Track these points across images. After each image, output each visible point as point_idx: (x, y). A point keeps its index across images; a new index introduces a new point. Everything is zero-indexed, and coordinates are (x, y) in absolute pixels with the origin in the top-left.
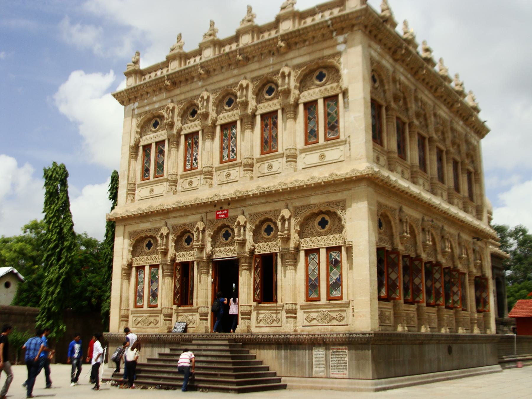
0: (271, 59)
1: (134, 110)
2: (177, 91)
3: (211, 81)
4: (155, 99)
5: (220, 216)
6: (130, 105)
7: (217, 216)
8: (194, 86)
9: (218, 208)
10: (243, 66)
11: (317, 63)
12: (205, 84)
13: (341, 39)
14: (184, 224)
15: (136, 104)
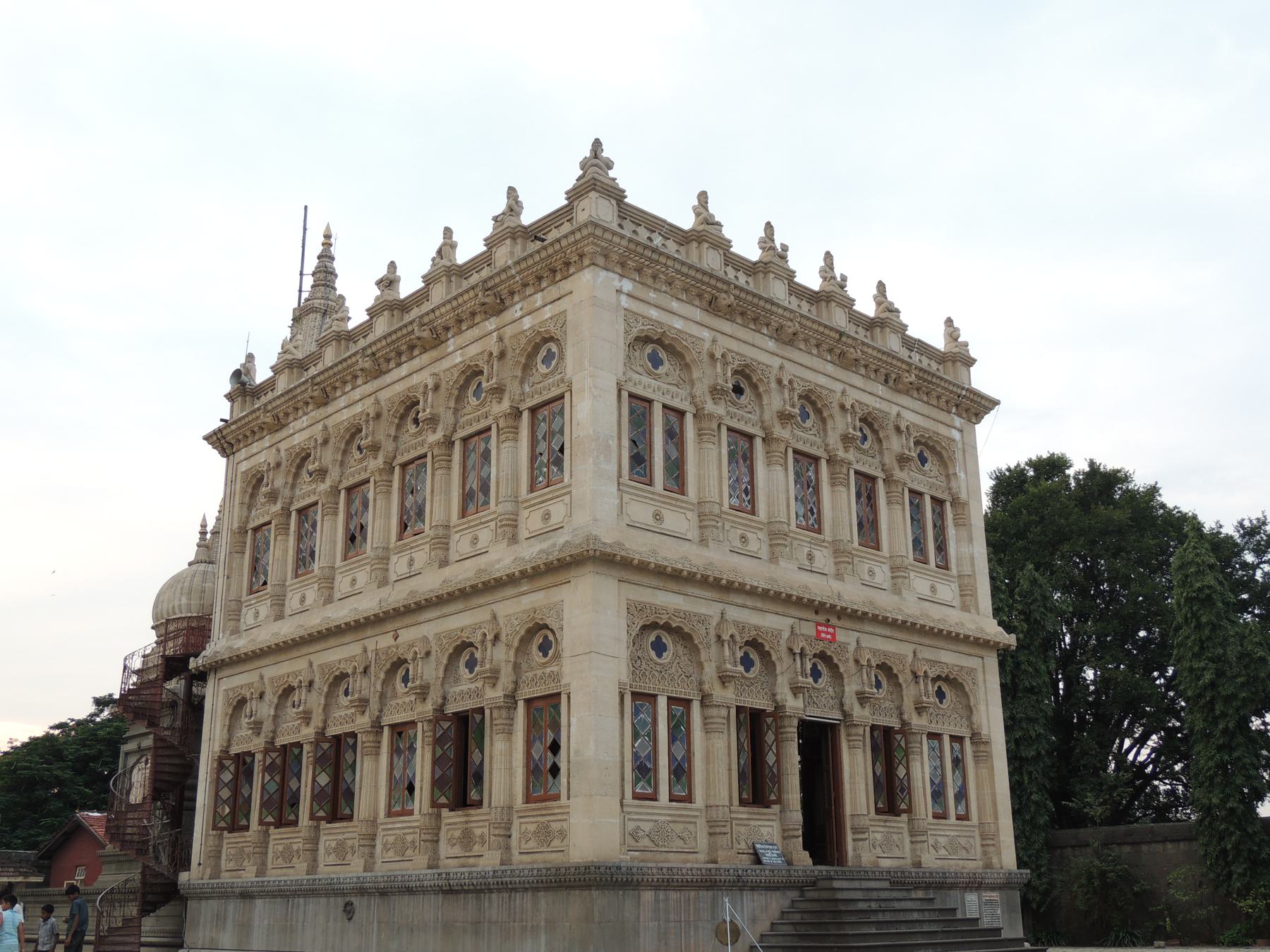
0: (881, 387)
1: (619, 291)
2: (726, 326)
3: (791, 357)
4: (675, 305)
5: (823, 635)
6: (611, 275)
7: (819, 632)
8: (758, 339)
9: (821, 618)
10: (846, 367)
11: (930, 438)
12: (779, 352)
13: (958, 422)
14: (757, 628)
15: (627, 285)
